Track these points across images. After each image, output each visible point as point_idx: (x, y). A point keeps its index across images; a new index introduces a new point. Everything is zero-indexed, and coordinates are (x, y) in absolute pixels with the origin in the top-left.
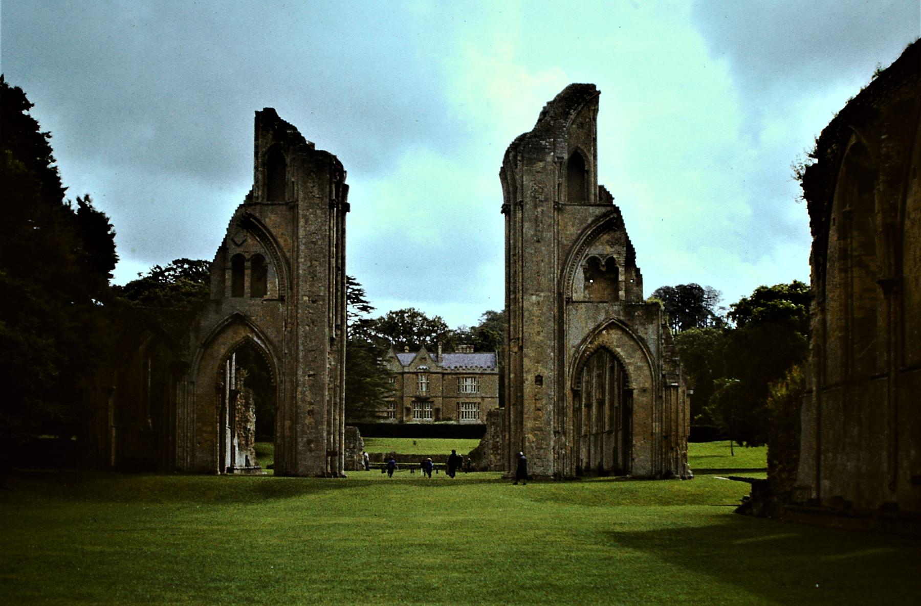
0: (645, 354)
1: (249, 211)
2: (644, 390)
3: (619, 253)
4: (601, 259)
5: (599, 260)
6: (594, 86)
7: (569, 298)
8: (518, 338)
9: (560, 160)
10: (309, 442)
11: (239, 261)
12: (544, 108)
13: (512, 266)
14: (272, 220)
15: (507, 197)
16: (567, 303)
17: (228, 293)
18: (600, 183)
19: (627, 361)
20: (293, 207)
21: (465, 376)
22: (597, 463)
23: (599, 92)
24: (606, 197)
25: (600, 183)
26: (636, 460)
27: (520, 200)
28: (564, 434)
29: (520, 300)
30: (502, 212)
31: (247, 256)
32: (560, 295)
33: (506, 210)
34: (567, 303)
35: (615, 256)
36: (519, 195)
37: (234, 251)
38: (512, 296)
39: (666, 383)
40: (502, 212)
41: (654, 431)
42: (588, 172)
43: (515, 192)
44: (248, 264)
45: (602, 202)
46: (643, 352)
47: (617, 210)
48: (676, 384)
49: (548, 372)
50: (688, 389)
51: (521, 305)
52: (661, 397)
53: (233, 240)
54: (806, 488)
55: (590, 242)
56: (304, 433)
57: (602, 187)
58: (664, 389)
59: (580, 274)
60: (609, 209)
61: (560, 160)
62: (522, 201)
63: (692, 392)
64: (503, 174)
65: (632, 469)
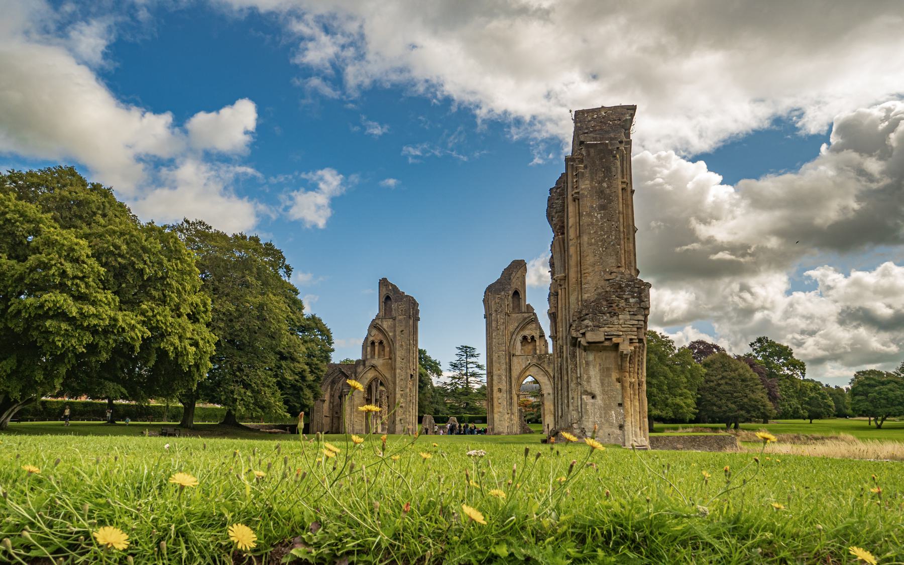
1: (377, 321)
2: (549, 394)
10: (401, 420)
11: (373, 343)
14: (386, 325)
17: (369, 357)
20: (394, 319)
28: (512, 414)
31: (376, 341)
32: (510, 353)
37: (371, 339)
47: (535, 314)
49: (504, 386)
55: (523, 329)
57: (528, 306)
59: (519, 344)
64: (484, 301)
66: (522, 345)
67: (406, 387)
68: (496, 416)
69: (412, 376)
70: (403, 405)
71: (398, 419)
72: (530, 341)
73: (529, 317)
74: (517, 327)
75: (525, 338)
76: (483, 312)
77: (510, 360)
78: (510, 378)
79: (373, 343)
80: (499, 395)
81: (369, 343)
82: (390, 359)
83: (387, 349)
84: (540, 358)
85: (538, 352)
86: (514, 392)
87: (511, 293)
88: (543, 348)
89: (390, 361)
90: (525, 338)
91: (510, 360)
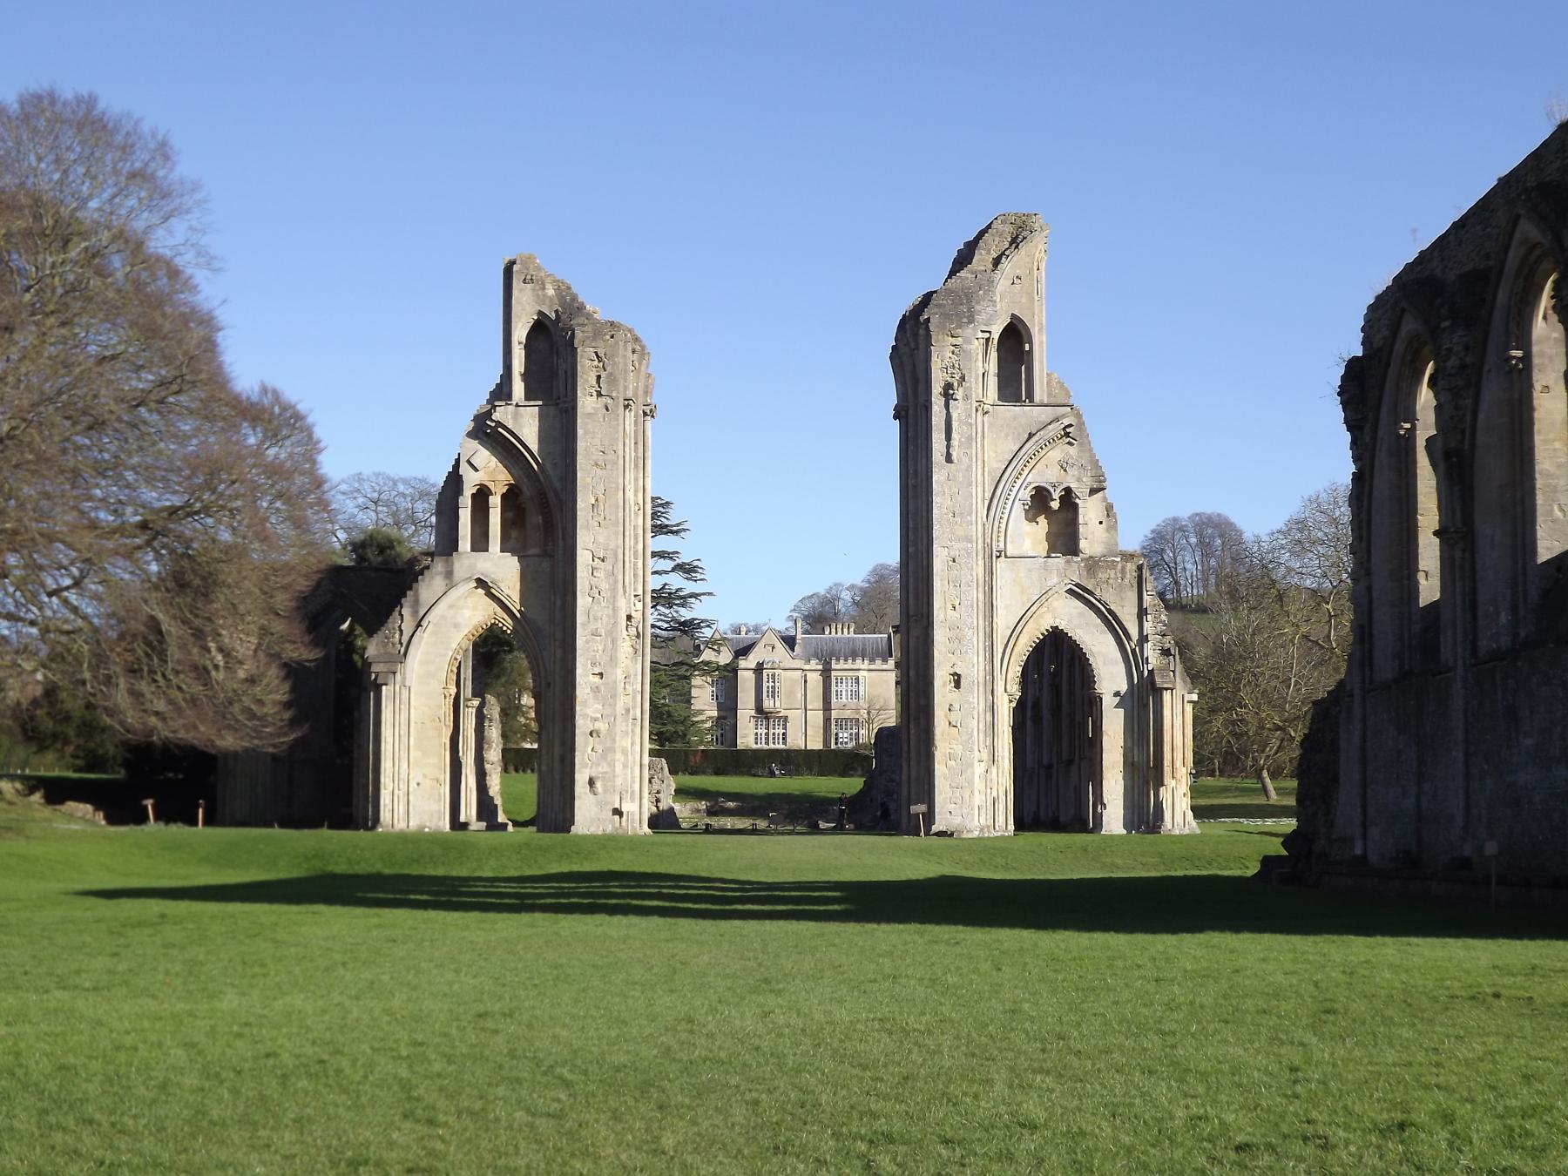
3: (1079, 480)
4: (1052, 491)
8: (922, 615)
9: (987, 335)
15: (902, 395)
17: (465, 543)
19: (1094, 649)
22: (1050, 814)
29: (925, 555)
30: (895, 417)
38: (911, 550)
40: (895, 417)
44: (495, 501)
45: (1052, 401)
51: (925, 563)
53: (469, 462)
56: (586, 766)
58: (1151, 692)
61: (987, 335)
63: (1195, 697)
64: (896, 356)
67: (613, 660)
69: (629, 618)
70: (601, 726)
71: (581, 778)
72: (1055, 505)
73: (1057, 420)
75: (1040, 497)
76: (889, 396)
77: (990, 572)
78: (990, 634)
79: (482, 494)
81: (466, 501)
82: (545, 554)
83: (535, 519)
84: (1093, 565)
85: (1083, 544)
87: (997, 331)
89: (546, 565)
90: (1040, 497)
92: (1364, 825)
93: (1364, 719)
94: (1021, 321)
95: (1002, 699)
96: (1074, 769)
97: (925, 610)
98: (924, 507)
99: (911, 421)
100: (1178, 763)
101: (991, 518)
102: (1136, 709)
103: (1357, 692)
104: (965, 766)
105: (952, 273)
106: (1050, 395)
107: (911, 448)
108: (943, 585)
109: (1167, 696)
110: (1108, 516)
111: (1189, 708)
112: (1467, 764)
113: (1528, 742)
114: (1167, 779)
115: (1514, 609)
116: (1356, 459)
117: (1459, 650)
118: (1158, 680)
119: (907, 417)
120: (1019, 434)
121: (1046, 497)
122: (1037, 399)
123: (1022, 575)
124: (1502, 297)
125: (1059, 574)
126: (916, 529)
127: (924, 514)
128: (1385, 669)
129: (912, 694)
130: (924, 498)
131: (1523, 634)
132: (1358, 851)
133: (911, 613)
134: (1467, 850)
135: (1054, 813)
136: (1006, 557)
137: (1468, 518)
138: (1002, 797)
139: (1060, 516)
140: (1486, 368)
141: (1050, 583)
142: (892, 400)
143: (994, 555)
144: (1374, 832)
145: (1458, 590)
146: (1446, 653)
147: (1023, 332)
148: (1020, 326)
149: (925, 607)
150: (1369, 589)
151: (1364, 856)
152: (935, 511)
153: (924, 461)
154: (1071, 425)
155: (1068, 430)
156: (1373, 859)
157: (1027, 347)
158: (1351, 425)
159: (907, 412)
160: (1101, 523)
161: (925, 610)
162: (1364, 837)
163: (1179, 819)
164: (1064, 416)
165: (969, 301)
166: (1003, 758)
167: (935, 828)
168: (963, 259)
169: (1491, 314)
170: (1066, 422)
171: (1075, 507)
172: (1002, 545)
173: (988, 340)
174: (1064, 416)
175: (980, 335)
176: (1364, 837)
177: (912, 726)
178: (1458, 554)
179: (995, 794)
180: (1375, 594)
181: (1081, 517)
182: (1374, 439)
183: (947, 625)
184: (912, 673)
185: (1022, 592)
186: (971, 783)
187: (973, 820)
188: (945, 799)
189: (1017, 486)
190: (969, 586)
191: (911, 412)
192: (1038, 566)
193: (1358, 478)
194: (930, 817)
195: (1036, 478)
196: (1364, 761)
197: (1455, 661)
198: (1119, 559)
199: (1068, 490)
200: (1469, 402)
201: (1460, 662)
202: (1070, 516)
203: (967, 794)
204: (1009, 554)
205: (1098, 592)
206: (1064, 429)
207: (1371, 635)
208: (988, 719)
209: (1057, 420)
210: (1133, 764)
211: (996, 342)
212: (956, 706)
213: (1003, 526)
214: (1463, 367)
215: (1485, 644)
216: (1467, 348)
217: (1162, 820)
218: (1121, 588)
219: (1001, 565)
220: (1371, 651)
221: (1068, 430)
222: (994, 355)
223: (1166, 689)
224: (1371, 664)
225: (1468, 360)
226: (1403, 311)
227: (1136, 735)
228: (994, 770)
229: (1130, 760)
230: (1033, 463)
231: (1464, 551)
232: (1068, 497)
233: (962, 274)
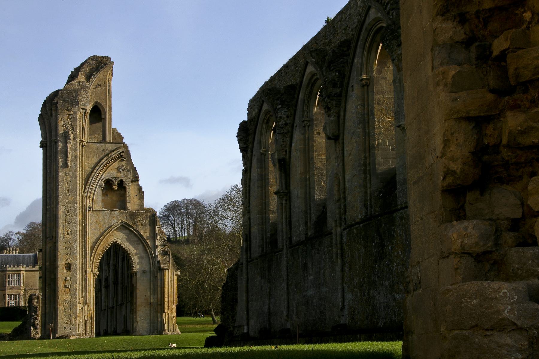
0: (145, 248)
3: (127, 176)
4: (114, 181)
5: (112, 181)
6: (108, 58)
7: (90, 208)
8: (53, 237)
9: (84, 111)
12: (72, 72)
13: (48, 185)
16: (89, 211)
18: (113, 126)
21: (11, 273)
22: (113, 329)
23: (113, 63)
24: (118, 138)
25: (113, 126)
26: (139, 323)
27: (55, 138)
29: (54, 209)
30: (41, 147)
33: (42, 145)
34: (89, 211)
35: (123, 179)
36: (53, 133)
38: (48, 207)
39: (160, 267)
40: (41, 147)
41: (152, 301)
42: (105, 119)
43: (51, 132)
45: (115, 141)
46: (144, 246)
47: (126, 147)
48: (167, 268)
50: (176, 271)
51: (54, 213)
52: (157, 277)
54: (240, 326)
57: (114, 130)
58: (159, 271)
60: (119, 145)
61: (84, 111)
62: (56, 139)
63: (179, 273)
64: (42, 119)
65: (136, 329)
66: (103, 195)
68: (60, 308)
72: (115, 187)
73: (117, 149)
74: (97, 164)
75: (108, 183)
76: (37, 136)
77: (85, 217)
80: (67, 273)
84: (132, 215)
85: (128, 205)
86: (89, 270)
87: (89, 108)
88: (136, 200)
90: (108, 183)
91: (85, 217)
92: (248, 319)
93: (247, 273)
94: (101, 105)
95: (90, 275)
96: (124, 307)
97: (54, 235)
98: (54, 188)
99: (48, 148)
100: (171, 303)
101: (86, 193)
102: (152, 278)
103: (244, 262)
104: (73, 306)
105: (68, 82)
106: (113, 138)
107: (48, 160)
108: (63, 223)
109: (166, 272)
110: (140, 193)
111: (176, 278)
112: (288, 289)
113: (312, 277)
114: (166, 310)
115: (306, 223)
116: (244, 164)
117: (285, 242)
118: (162, 265)
119: (46, 147)
120: (99, 156)
121: (111, 184)
122: (108, 140)
123: (100, 218)
124: (301, 95)
125: (117, 218)
126: (50, 197)
127: (54, 191)
128: (256, 252)
129: (47, 273)
130: (54, 183)
131: (309, 234)
132: (245, 331)
133: (47, 236)
134: (289, 326)
135: (114, 328)
136: (93, 210)
137: (287, 185)
138: (90, 320)
139: (118, 192)
140: (295, 125)
141: (113, 223)
142: (38, 138)
143: (86, 210)
144: (252, 322)
145: (284, 217)
146: (279, 245)
147: (101, 110)
148: (100, 107)
149: (54, 233)
150: (249, 219)
151: (248, 332)
152: (60, 189)
153: (54, 166)
154: (123, 152)
155: (122, 154)
156: (251, 334)
157: (103, 117)
158: (242, 149)
159: (46, 145)
160: (136, 196)
161: (54, 235)
162: (248, 325)
163: (171, 328)
164: (120, 147)
165: (76, 95)
166: (90, 302)
167: (57, 335)
168: (73, 76)
169: (297, 102)
170: (121, 150)
171: (125, 188)
172: (91, 205)
173: (85, 113)
174: (120, 147)
175: (81, 110)
176: (248, 325)
177: (47, 288)
178: (284, 202)
179: (86, 318)
180: (252, 221)
181: (127, 193)
182: (252, 155)
183: (65, 241)
184: (48, 264)
185: (100, 226)
186: (75, 314)
187: (76, 331)
188: (62, 321)
189: (98, 179)
190: (76, 223)
191: (48, 144)
192: (107, 215)
193: (245, 172)
194: (55, 331)
195: (106, 175)
196: (247, 292)
197: (283, 246)
198: (144, 212)
199: (122, 181)
200: (288, 139)
201: (285, 246)
202: (122, 192)
203: (73, 319)
204: (94, 209)
205: (134, 227)
206: (120, 154)
207: (250, 238)
208: (83, 284)
209: (117, 149)
210: (150, 304)
211: (89, 114)
212: (69, 278)
213: (92, 196)
214: (286, 124)
215: (295, 239)
216: (288, 117)
217: (164, 328)
218: (145, 225)
219: (90, 214)
220: (250, 245)
221: (122, 154)
222: (87, 119)
223: (165, 269)
224: (250, 250)
225: (288, 122)
226: (263, 101)
227: (152, 290)
228: (86, 308)
229: (149, 301)
230: (105, 168)
231: (286, 200)
232: (121, 184)
233: (73, 82)
